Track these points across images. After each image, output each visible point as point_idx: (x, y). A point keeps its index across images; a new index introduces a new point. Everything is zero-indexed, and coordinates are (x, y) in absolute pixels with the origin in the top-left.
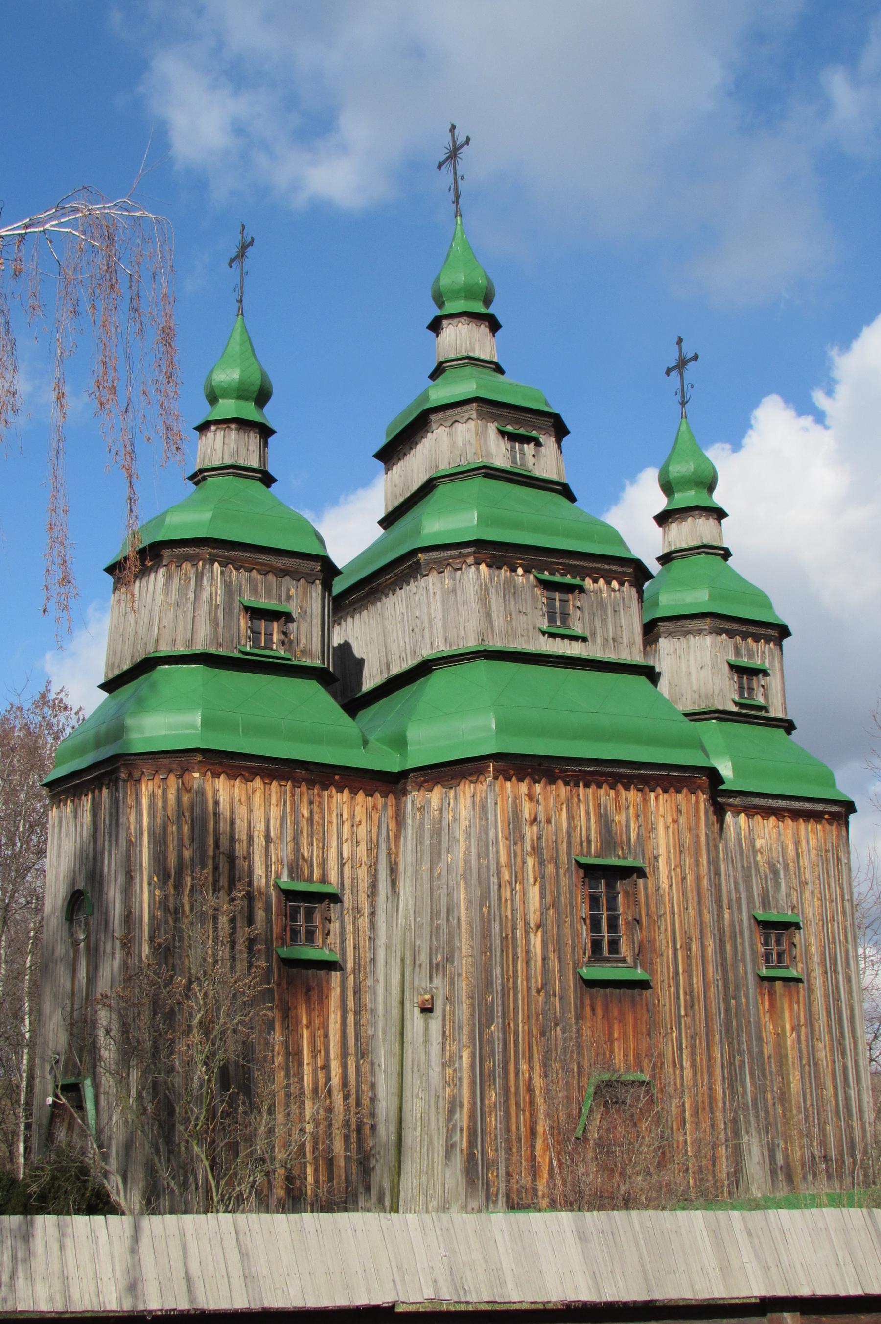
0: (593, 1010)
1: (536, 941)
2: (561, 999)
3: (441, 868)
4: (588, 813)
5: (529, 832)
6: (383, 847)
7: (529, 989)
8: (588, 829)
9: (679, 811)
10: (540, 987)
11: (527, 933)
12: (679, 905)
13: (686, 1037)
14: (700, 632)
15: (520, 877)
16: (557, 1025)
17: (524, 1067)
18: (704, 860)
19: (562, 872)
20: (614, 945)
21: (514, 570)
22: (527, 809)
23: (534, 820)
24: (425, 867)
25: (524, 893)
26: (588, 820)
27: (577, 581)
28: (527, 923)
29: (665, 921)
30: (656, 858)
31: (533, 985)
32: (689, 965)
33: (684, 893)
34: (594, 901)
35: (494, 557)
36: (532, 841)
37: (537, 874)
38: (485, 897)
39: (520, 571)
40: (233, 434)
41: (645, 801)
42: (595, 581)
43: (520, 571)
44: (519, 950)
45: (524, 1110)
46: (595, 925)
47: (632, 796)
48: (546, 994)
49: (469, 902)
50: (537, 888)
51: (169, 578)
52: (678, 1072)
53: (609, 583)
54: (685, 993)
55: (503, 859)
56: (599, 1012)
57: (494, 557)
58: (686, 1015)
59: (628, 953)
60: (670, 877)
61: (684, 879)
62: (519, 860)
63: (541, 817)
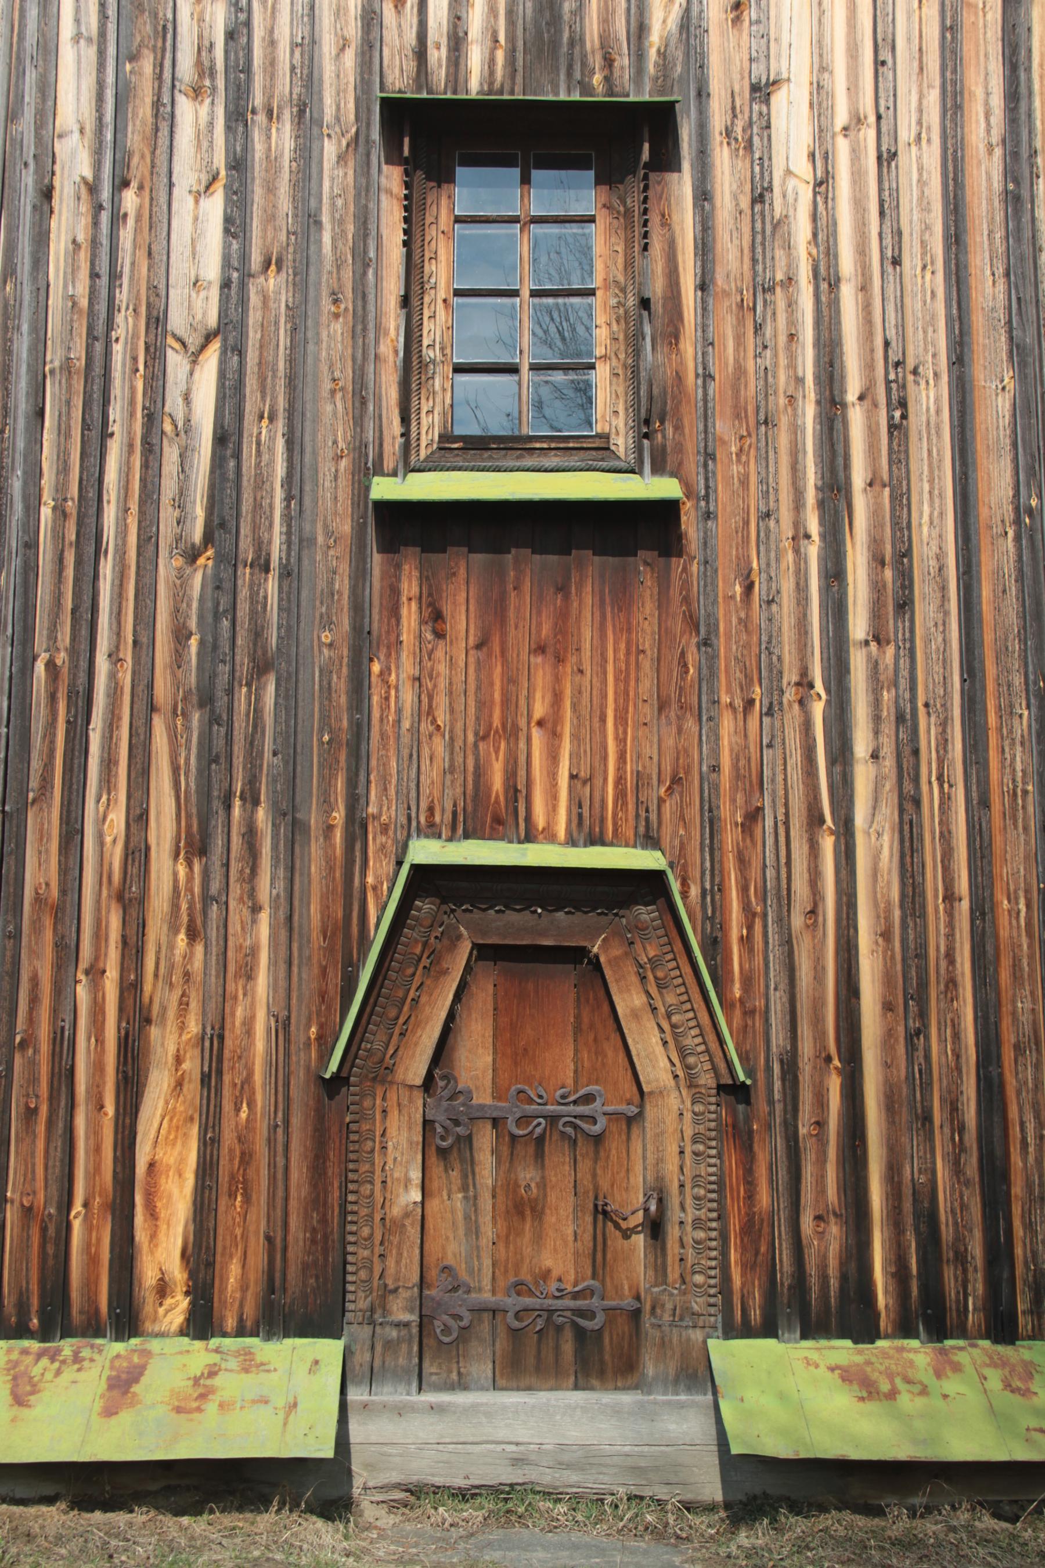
2: (286, 573)
7: (148, 540)
10: (197, 535)
11: (155, 354)
12: (861, 251)
13: (877, 719)
15: (138, 169)
16: (261, 667)
19: (330, 150)
29: (791, 304)
31: (167, 529)
32: (899, 456)
36: (203, 47)
37: (220, 160)
44: (116, 413)
45: (96, 973)
48: (219, 558)
50: (215, 206)
52: (828, 844)
54: (878, 560)
58: (878, 637)
59: (620, 422)
61: (886, 158)
62: (143, 109)
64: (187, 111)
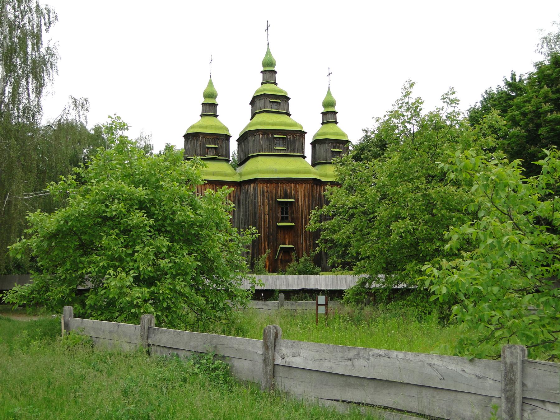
0: (281, 232)
1: (267, 218)
3: (247, 202)
4: (281, 189)
5: (266, 194)
6: (237, 197)
8: (281, 193)
9: (305, 188)
14: (325, 143)
16: (271, 235)
17: (263, 244)
18: (311, 199)
20: (287, 218)
21: (269, 135)
22: (266, 189)
23: (267, 192)
24: (244, 202)
25: (264, 207)
26: (281, 191)
27: (285, 136)
28: (264, 214)
30: (298, 199)
33: (305, 206)
34: (282, 209)
35: (263, 132)
38: (255, 208)
39: (270, 135)
40: (208, 106)
41: (296, 186)
42: (290, 136)
43: (270, 135)
46: (282, 213)
47: (293, 185)
49: (252, 209)
51: (191, 141)
53: (293, 136)
55: (259, 200)
56: (282, 232)
57: (263, 132)
60: (302, 203)
63: (269, 191)
64: (266, 201)
